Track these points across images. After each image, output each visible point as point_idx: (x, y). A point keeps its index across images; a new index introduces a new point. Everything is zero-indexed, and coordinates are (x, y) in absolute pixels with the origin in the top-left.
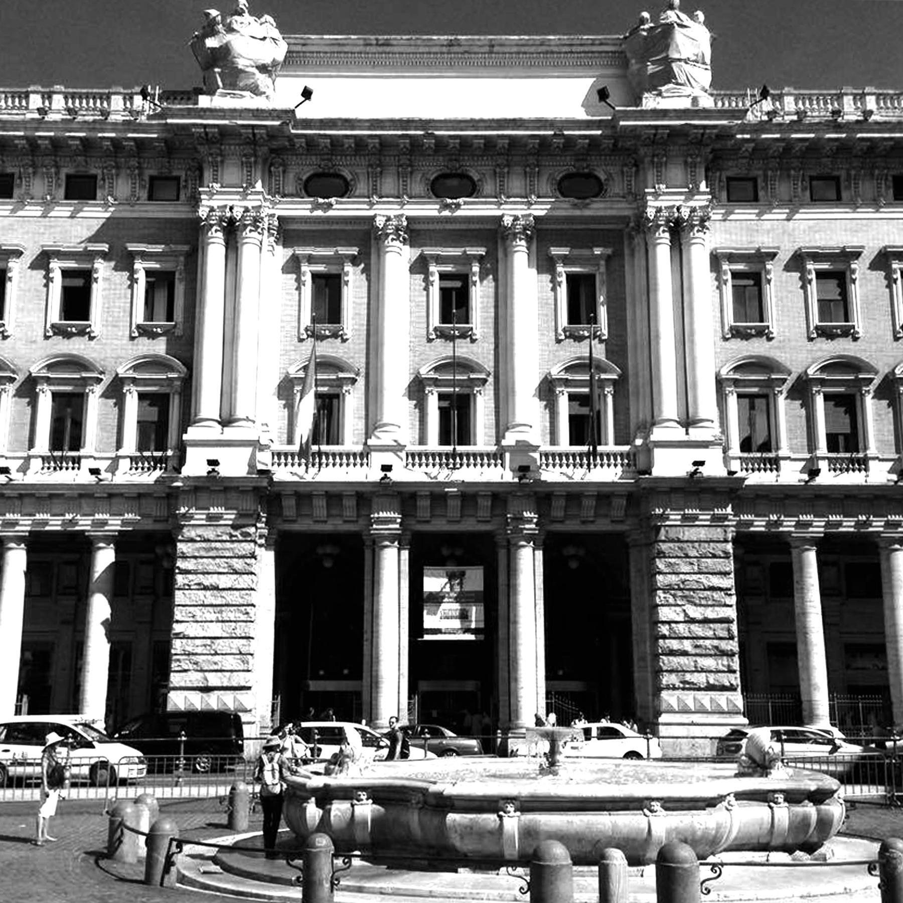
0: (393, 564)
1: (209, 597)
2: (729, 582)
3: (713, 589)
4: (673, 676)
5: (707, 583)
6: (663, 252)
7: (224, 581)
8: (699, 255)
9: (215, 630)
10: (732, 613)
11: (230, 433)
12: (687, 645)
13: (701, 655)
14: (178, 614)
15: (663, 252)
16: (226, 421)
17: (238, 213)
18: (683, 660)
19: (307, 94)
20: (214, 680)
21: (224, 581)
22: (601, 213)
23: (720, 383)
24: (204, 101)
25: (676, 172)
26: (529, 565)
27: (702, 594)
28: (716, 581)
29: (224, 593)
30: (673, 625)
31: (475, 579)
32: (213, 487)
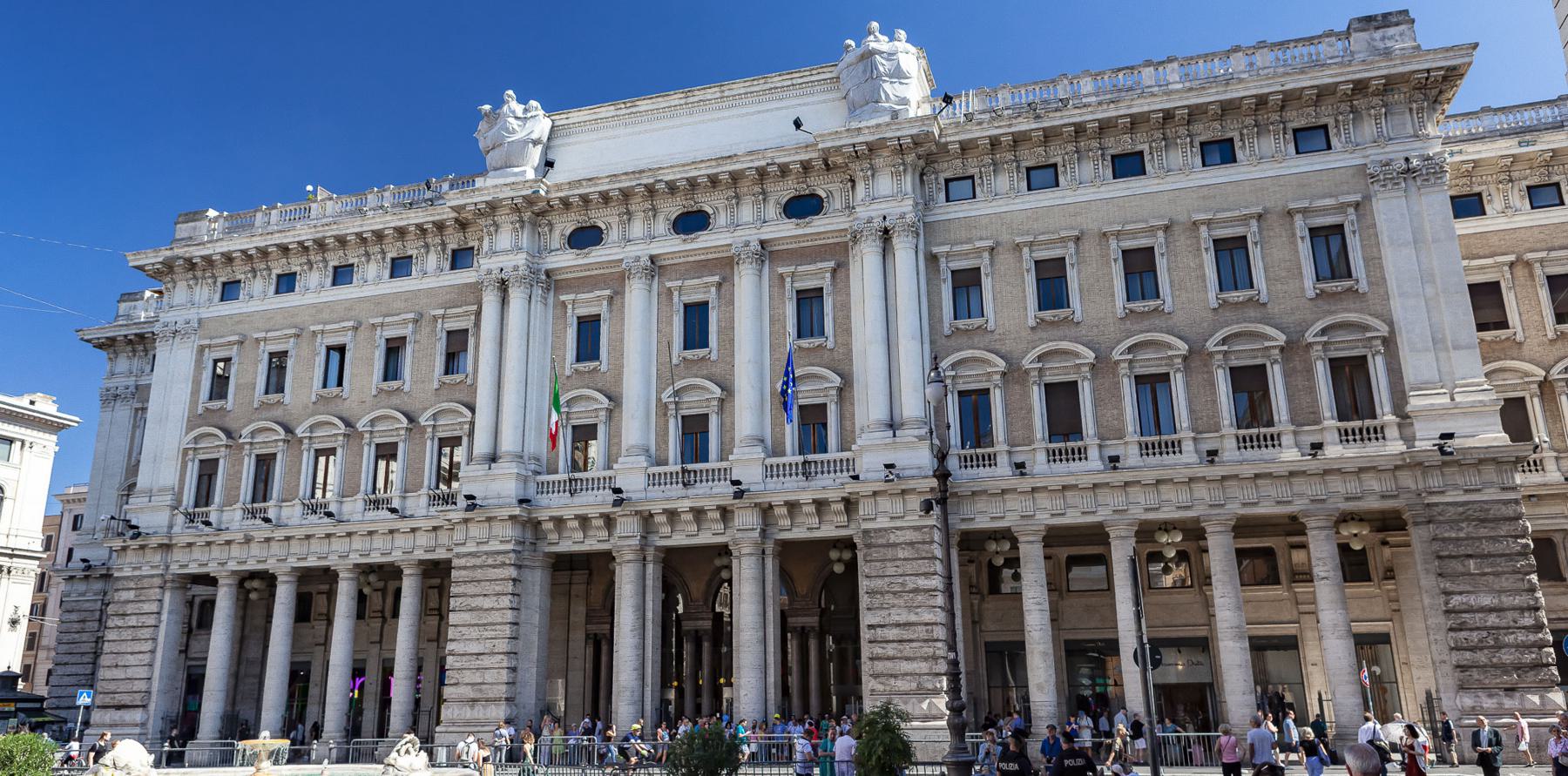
3: (916, 591)
4: (883, 679)
5: (911, 586)
7: (487, 603)
12: (890, 650)
13: (907, 659)
14: (451, 633)
18: (889, 664)
21: (487, 603)
22: (822, 229)
27: (906, 597)
28: (922, 582)
29: (485, 614)
30: (879, 630)
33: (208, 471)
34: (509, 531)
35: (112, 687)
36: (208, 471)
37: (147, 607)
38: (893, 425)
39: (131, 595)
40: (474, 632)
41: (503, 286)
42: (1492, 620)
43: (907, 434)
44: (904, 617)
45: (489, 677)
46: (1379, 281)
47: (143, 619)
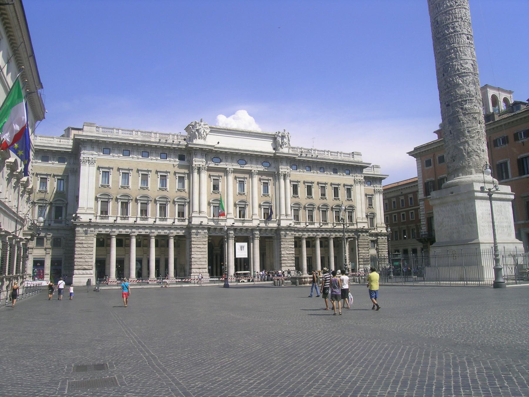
0: (231, 242)
1: (198, 250)
2: (293, 246)
6: (282, 181)
7: (202, 246)
8: (288, 181)
9: (200, 256)
10: (294, 252)
11: (201, 215)
12: (286, 258)
14: (193, 253)
15: (282, 181)
16: (200, 212)
17: (201, 166)
19: (218, 143)
20: (200, 267)
21: (202, 246)
23: (291, 207)
24: (195, 141)
25: (284, 163)
26: (257, 242)
31: (245, 244)
32: (200, 227)
33: (105, 204)
34: (206, 231)
35: (81, 264)
36: (105, 204)
37: (90, 242)
38: (286, 215)
39: (84, 238)
40: (198, 253)
41: (199, 169)
42: (364, 255)
43: (288, 218)
44: (288, 252)
45: (203, 263)
46: (354, 199)
47: (89, 245)
